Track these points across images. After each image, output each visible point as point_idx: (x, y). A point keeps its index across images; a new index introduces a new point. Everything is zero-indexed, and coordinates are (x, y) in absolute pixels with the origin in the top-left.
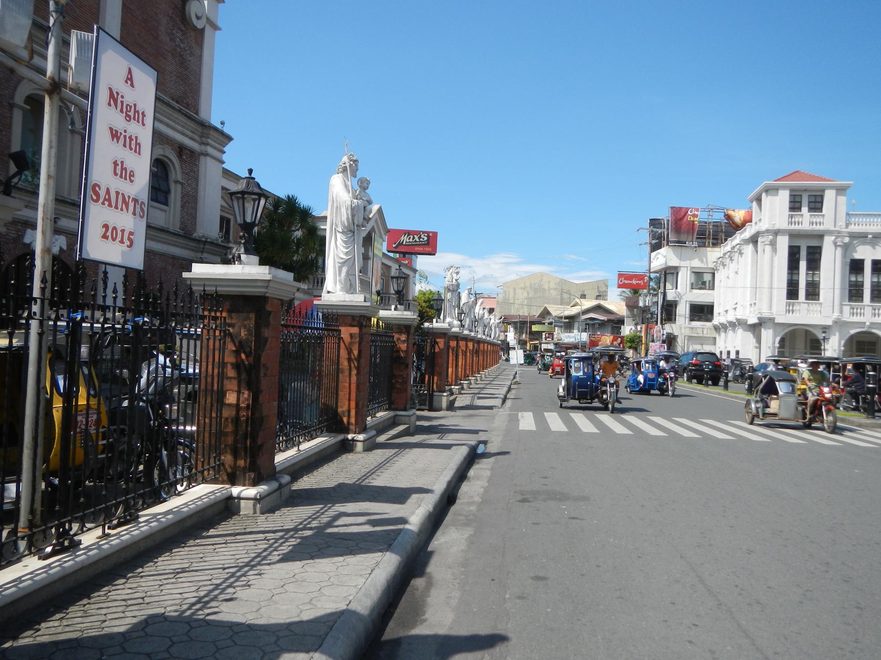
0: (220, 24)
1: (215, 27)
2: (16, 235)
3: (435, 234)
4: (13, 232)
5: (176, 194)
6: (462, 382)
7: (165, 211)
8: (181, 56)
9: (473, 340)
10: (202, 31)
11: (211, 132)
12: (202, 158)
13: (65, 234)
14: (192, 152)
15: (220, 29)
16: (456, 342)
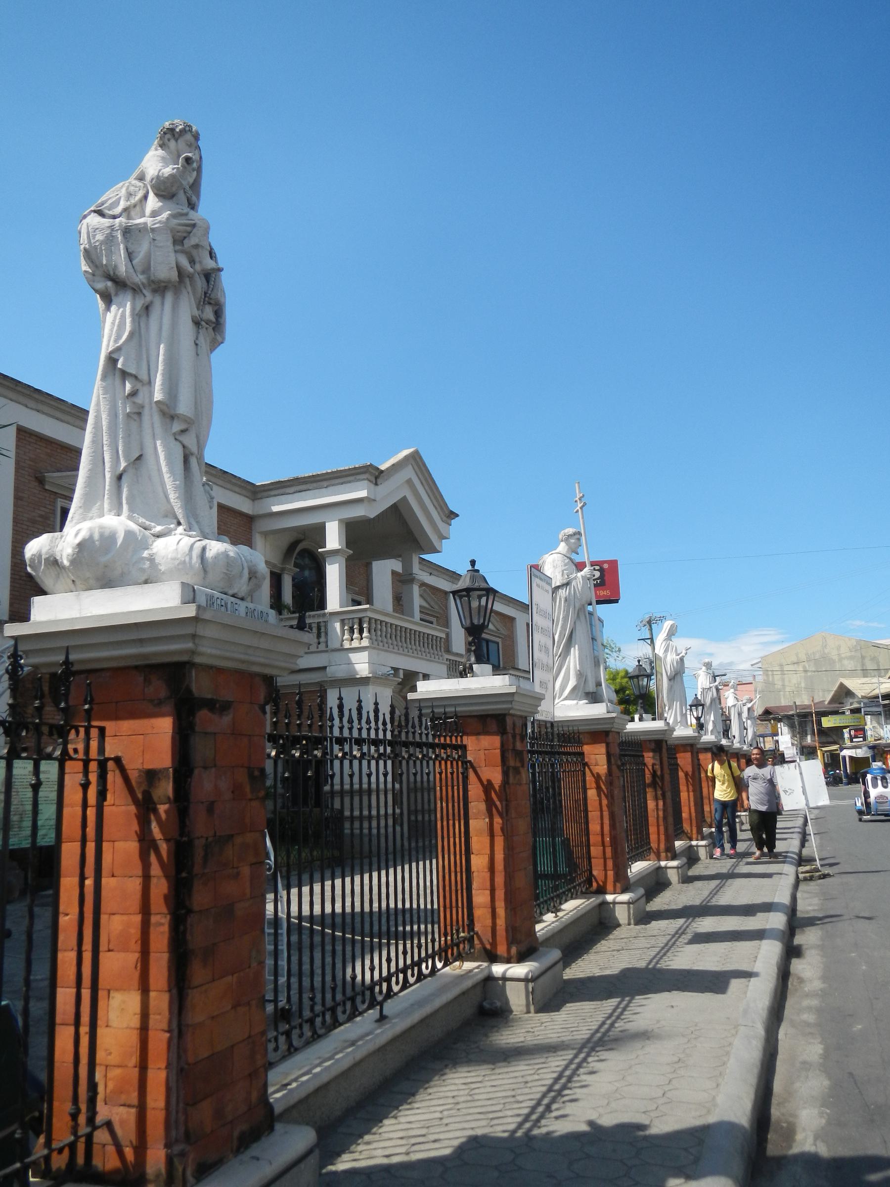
3: (614, 564)
6: (498, 969)
9: (607, 733)
16: (164, 725)
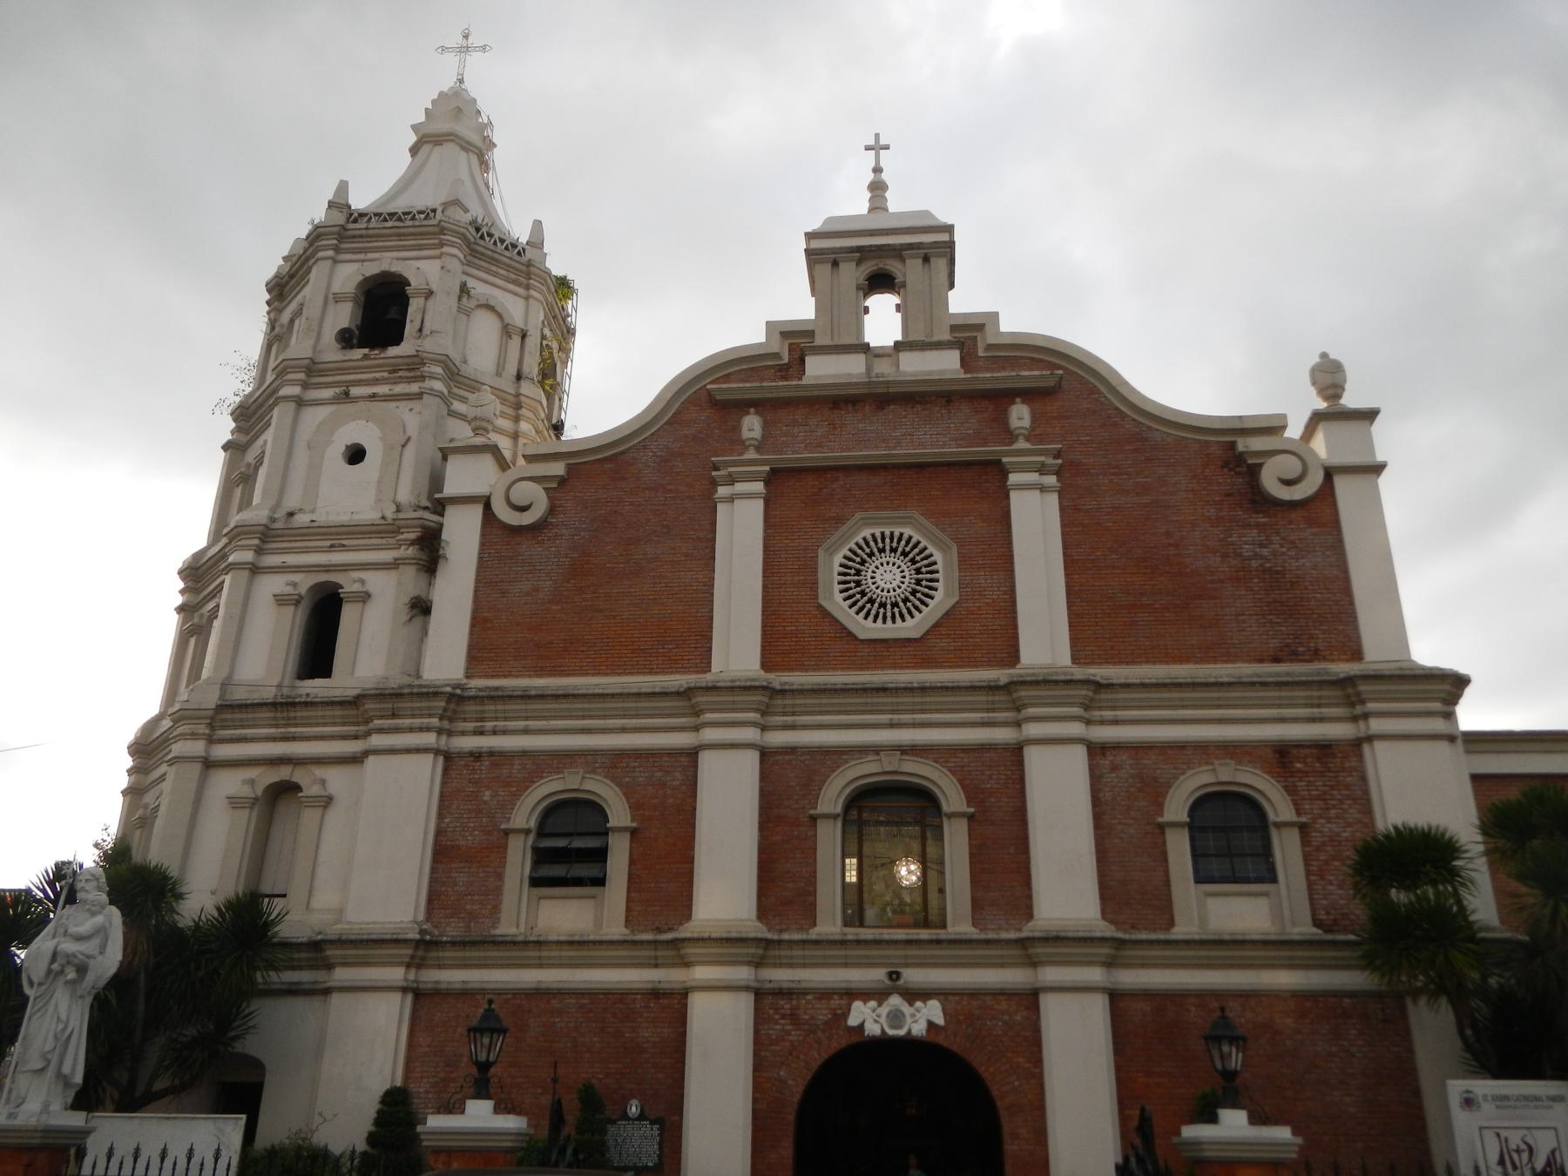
2: (830, 1016)
4: (826, 1012)
7: (1266, 894)
12: (1366, 748)
13: (942, 997)
14: (1324, 749)
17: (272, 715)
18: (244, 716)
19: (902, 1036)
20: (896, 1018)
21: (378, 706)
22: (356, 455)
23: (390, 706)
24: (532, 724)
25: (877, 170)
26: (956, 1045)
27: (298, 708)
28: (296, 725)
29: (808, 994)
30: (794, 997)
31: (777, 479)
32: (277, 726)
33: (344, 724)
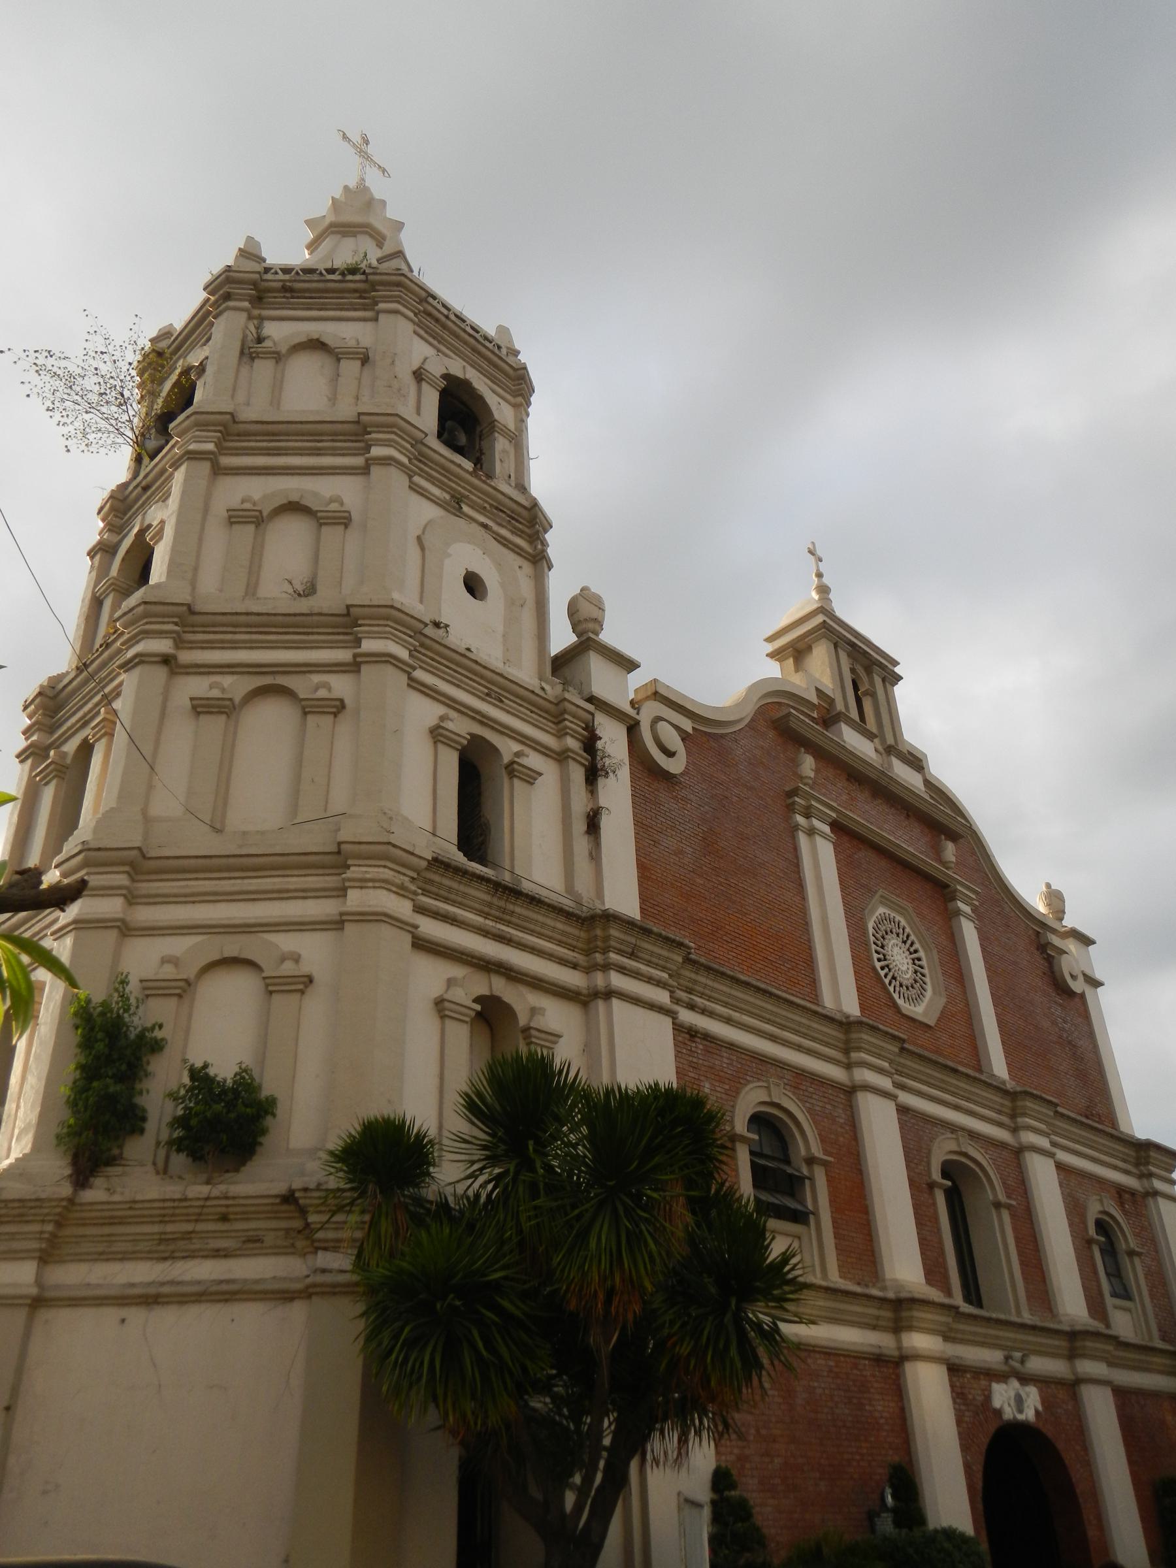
0: (1099, 975)
1: (1096, 984)
5: (1136, 1273)
8: (1070, 1042)
10: (1082, 996)
11: (1152, 1154)
14: (1133, 1193)
15: (1101, 984)
17: (487, 898)
18: (455, 885)
19: (1022, 1420)
20: (1019, 1401)
21: (622, 936)
22: (473, 585)
23: (633, 940)
24: (736, 1015)
25: (819, 575)
26: (1048, 1430)
27: (519, 902)
28: (509, 923)
29: (965, 1371)
30: (960, 1374)
31: (836, 826)
32: (486, 916)
33: (560, 943)
